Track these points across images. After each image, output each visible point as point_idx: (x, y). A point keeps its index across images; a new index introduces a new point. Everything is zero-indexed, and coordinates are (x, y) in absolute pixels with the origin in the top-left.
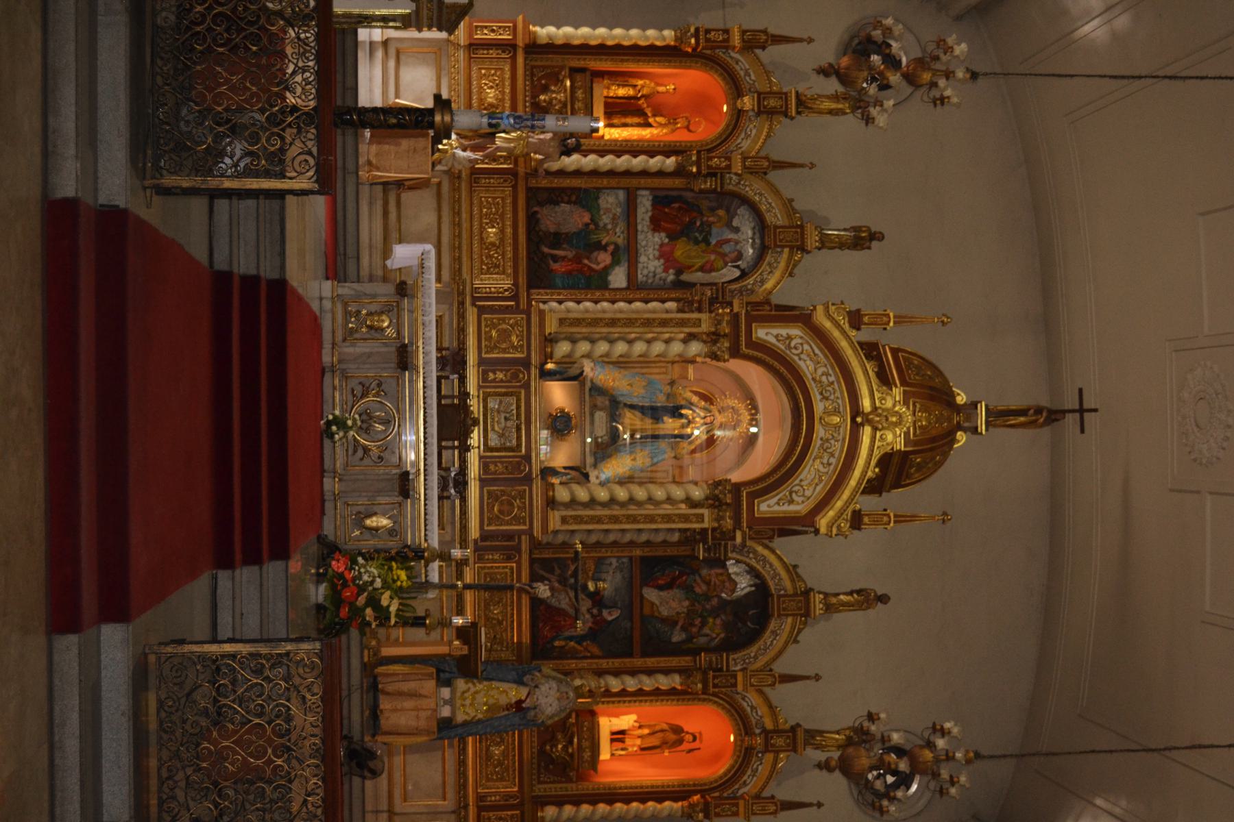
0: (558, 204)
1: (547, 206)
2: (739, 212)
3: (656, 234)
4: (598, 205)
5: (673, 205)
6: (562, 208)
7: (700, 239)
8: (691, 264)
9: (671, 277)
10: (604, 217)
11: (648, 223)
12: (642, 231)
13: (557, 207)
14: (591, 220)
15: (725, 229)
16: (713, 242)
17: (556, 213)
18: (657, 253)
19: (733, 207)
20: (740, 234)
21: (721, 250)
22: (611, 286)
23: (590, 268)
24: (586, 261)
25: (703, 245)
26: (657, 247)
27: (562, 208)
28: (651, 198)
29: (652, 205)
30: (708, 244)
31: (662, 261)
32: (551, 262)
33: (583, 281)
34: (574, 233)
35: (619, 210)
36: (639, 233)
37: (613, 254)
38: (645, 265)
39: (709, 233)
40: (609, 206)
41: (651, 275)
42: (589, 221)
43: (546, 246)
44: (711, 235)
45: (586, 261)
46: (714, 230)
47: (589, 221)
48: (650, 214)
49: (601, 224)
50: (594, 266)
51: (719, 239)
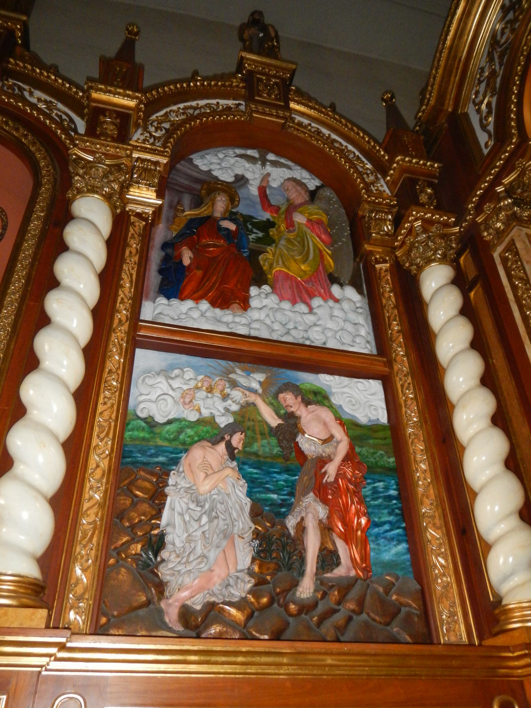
0: (162, 536)
1: (164, 572)
2: (204, 168)
3: (254, 303)
4: (169, 422)
5: (186, 262)
6: (178, 520)
7: (260, 235)
8: (317, 252)
9: (350, 292)
10: (206, 413)
11: (227, 312)
12: (248, 325)
13: (168, 539)
14: (215, 443)
15: (242, 193)
16: (266, 216)
17: (190, 539)
18: (302, 307)
19: (195, 174)
20: (248, 175)
21: (283, 208)
22: (384, 419)
23: (349, 458)
24: (331, 469)
25: (272, 232)
26: (286, 305)
27: (178, 520)
28: (162, 300)
29: (182, 299)
30: (269, 225)
31: (316, 302)
32: (340, 572)
33: (381, 484)
34: (249, 494)
35: (189, 374)
36: (253, 333)
37: (307, 403)
38: (329, 334)
39: (249, 218)
40: (177, 395)
41: (349, 327)
42: (222, 447)
43: (295, 584)
44: (251, 217)
45: (331, 469)
46: (242, 209)
47: (222, 447)
48: (204, 305)
49: (223, 421)
50: (343, 449)
51: (259, 207)
